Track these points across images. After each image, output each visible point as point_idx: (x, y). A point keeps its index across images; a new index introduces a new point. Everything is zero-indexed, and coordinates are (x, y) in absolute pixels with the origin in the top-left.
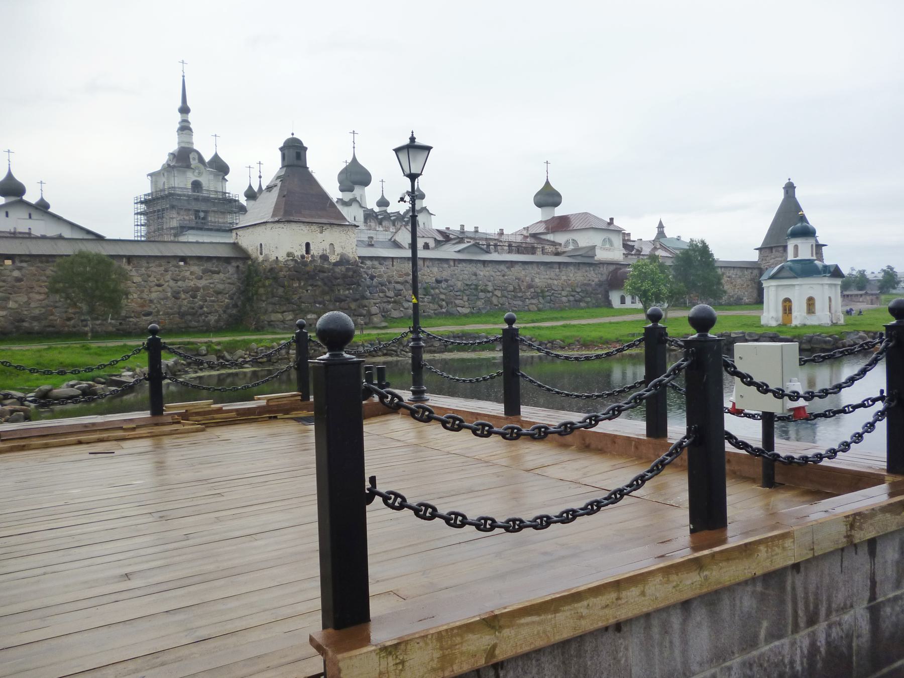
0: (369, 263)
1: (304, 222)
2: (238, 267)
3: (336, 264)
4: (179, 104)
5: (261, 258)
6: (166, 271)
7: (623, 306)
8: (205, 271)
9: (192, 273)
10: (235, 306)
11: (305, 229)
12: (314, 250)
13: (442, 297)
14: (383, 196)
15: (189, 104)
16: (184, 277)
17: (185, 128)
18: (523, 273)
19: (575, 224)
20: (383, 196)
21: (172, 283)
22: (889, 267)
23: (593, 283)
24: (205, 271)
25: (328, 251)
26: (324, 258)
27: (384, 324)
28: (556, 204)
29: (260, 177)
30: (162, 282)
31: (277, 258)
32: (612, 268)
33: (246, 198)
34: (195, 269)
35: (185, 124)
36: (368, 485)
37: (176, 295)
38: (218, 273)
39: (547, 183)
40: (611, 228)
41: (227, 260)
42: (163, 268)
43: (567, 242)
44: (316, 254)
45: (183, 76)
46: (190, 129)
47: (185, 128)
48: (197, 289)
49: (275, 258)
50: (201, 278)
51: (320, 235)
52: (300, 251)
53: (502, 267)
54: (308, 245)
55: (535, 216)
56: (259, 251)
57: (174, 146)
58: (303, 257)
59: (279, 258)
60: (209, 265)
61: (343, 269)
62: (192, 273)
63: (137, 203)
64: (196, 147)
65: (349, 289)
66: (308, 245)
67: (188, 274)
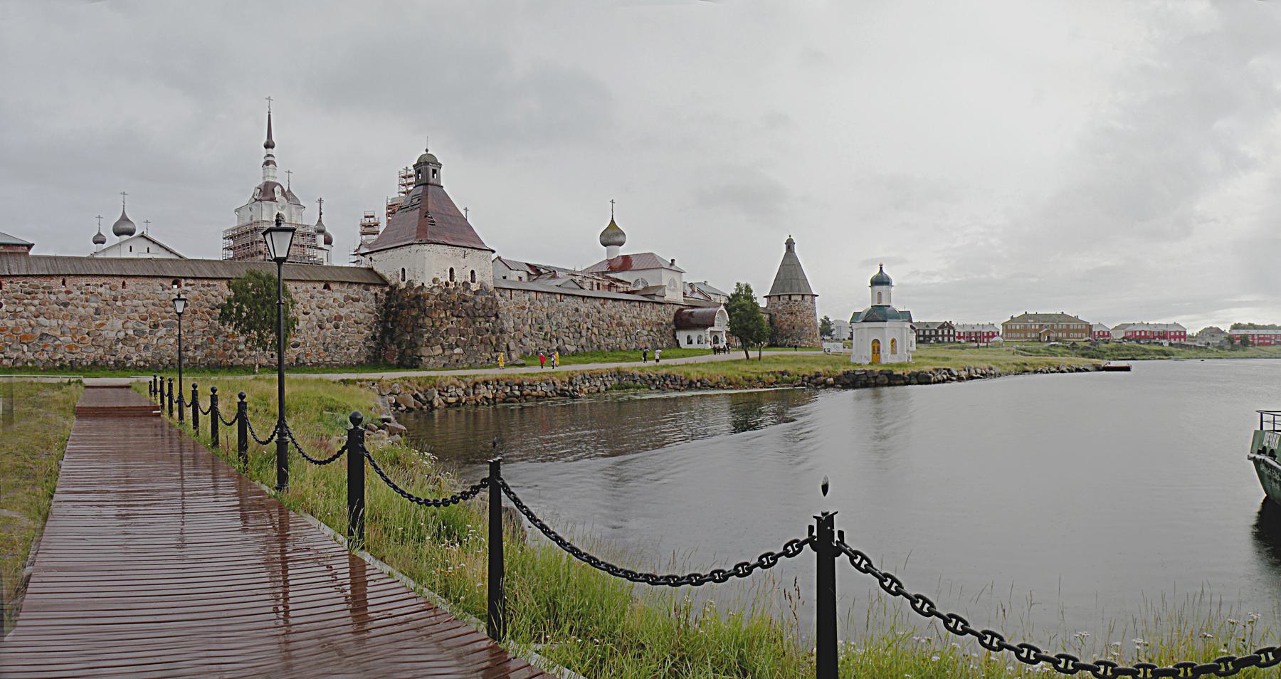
1: (448, 245)
2: (376, 294)
3: (476, 293)
4: (265, 140)
5: (403, 285)
6: (312, 297)
7: (690, 346)
8: (347, 298)
10: (374, 338)
16: (327, 304)
19: (635, 264)
22: (826, 318)
23: (664, 323)
27: (521, 362)
28: (621, 244)
30: (308, 309)
31: (423, 284)
32: (677, 308)
36: (836, 538)
38: (358, 300)
40: (673, 268)
42: (309, 295)
48: (339, 318)
49: (421, 285)
51: (462, 260)
55: (602, 254)
56: (400, 277)
58: (447, 284)
59: (425, 285)
63: (225, 238)
65: (488, 322)
67: (331, 301)
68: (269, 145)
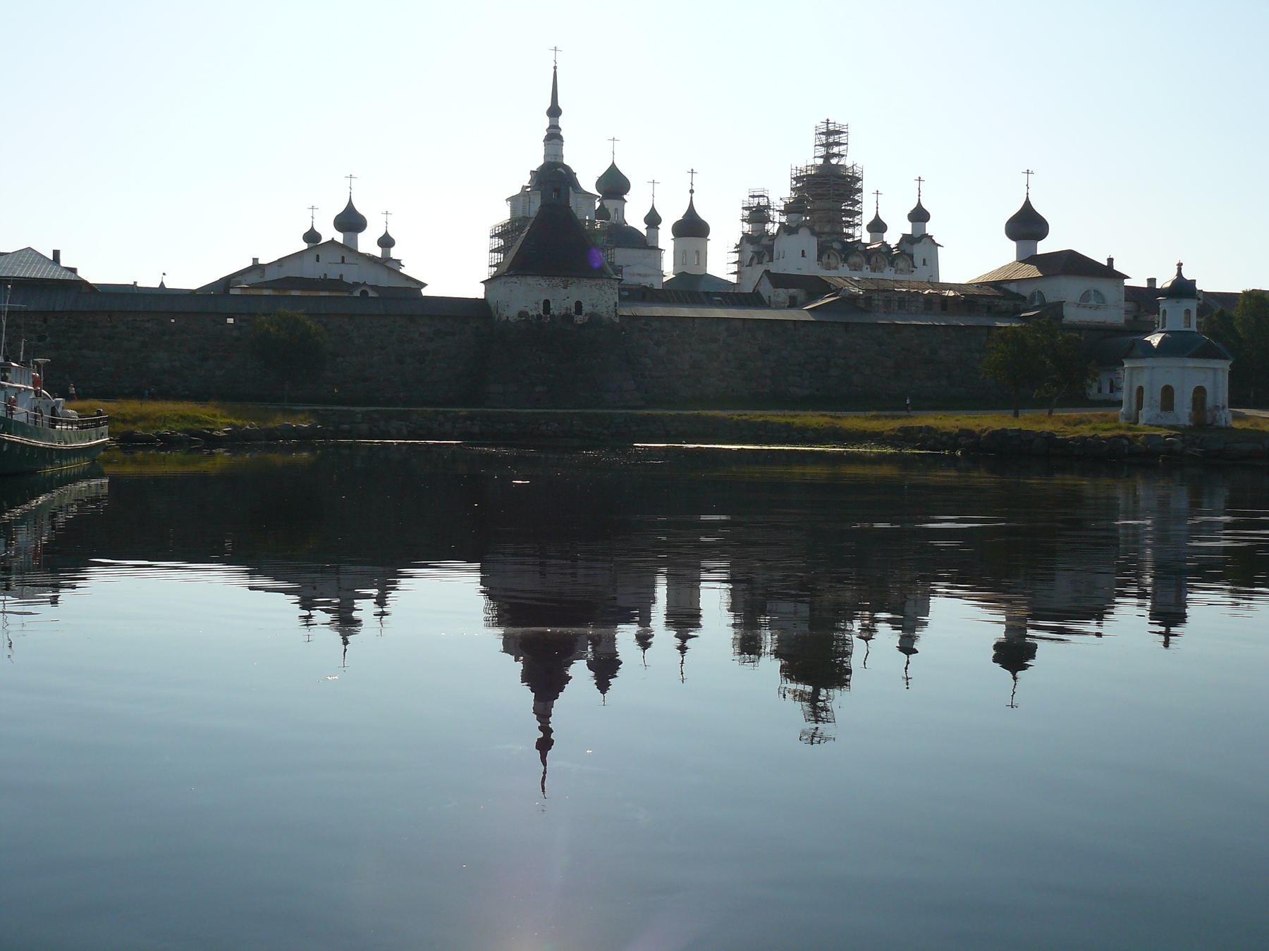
3: (582, 326)
4: (548, 104)
11: (544, 283)
12: (555, 310)
14: (877, 215)
15: (560, 104)
17: (554, 137)
20: (877, 215)
25: (573, 310)
26: (567, 318)
29: (692, 191)
31: (508, 317)
33: (647, 226)
35: (553, 131)
39: (1027, 203)
43: (1033, 295)
44: (556, 313)
45: (555, 68)
47: (554, 137)
51: (563, 291)
52: (535, 311)
54: (547, 303)
57: (537, 160)
58: (539, 317)
59: (510, 319)
64: (566, 161)
66: (547, 303)
68: (554, 112)
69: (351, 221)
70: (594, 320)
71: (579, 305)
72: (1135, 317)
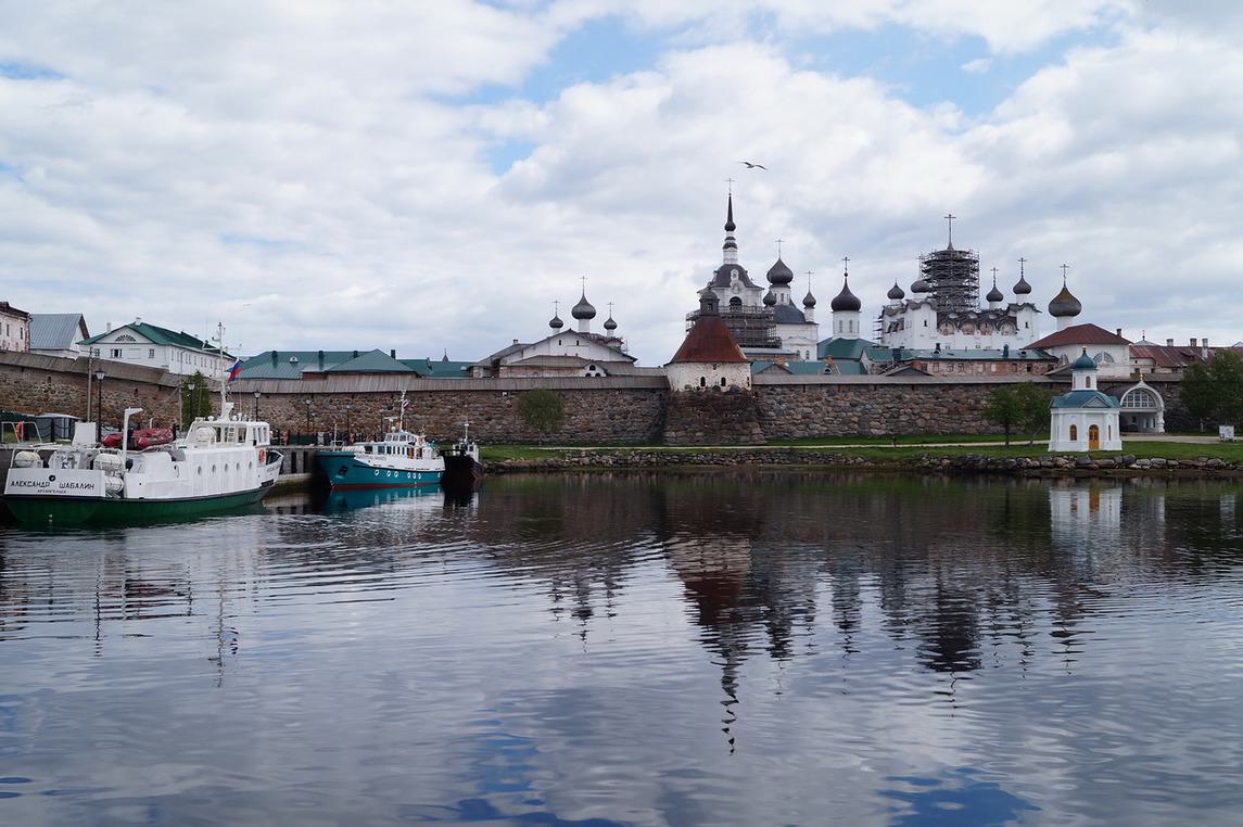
0: (779, 390)
8: (635, 399)
9: (625, 401)
13: (856, 419)
17: (730, 245)
18: (964, 395)
21: (609, 408)
24: (635, 399)
26: (716, 388)
28: (1075, 313)
29: (846, 275)
34: (627, 397)
37: (612, 417)
41: (653, 390)
46: (734, 246)
47: (730, 245)
50: (631, 404)
52: (696, 384)
53: (937, 390)
54: (703, 379)
58: (698, 388)
60: (638, 395)
61: (733, 397)
62: (625, 401)
66: (703, 379)
68: (730, 227)
69: (584, 312)
70: (734, 390)
71: (723, 380)
72: (1153, 370)
